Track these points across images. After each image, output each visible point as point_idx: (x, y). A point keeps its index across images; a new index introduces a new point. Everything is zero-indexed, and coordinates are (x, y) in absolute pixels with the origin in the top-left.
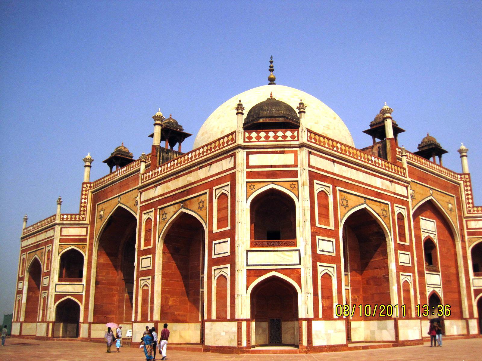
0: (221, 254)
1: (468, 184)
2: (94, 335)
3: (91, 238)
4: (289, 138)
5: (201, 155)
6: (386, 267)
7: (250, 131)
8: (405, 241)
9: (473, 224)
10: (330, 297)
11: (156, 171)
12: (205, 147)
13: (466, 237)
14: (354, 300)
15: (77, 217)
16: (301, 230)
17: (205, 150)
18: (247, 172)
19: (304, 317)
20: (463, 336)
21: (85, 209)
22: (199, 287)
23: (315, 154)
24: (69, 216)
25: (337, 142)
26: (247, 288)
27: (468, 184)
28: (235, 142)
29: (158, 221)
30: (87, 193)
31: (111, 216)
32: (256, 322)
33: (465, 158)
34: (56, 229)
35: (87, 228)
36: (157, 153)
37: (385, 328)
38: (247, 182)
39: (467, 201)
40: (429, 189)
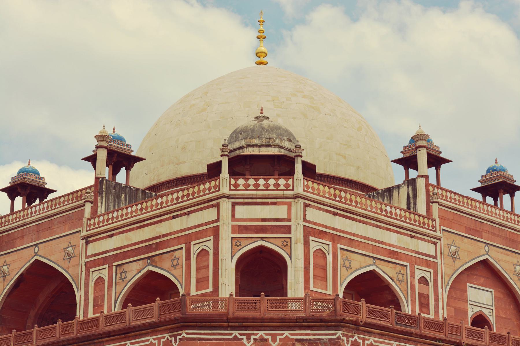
4: (282, 187)
5: (175, 202)
7: (237, 177)
11: (110, 216)
12: (181, 192)
28: (219, 190)
31: (22, 275)
38: (232, 238)
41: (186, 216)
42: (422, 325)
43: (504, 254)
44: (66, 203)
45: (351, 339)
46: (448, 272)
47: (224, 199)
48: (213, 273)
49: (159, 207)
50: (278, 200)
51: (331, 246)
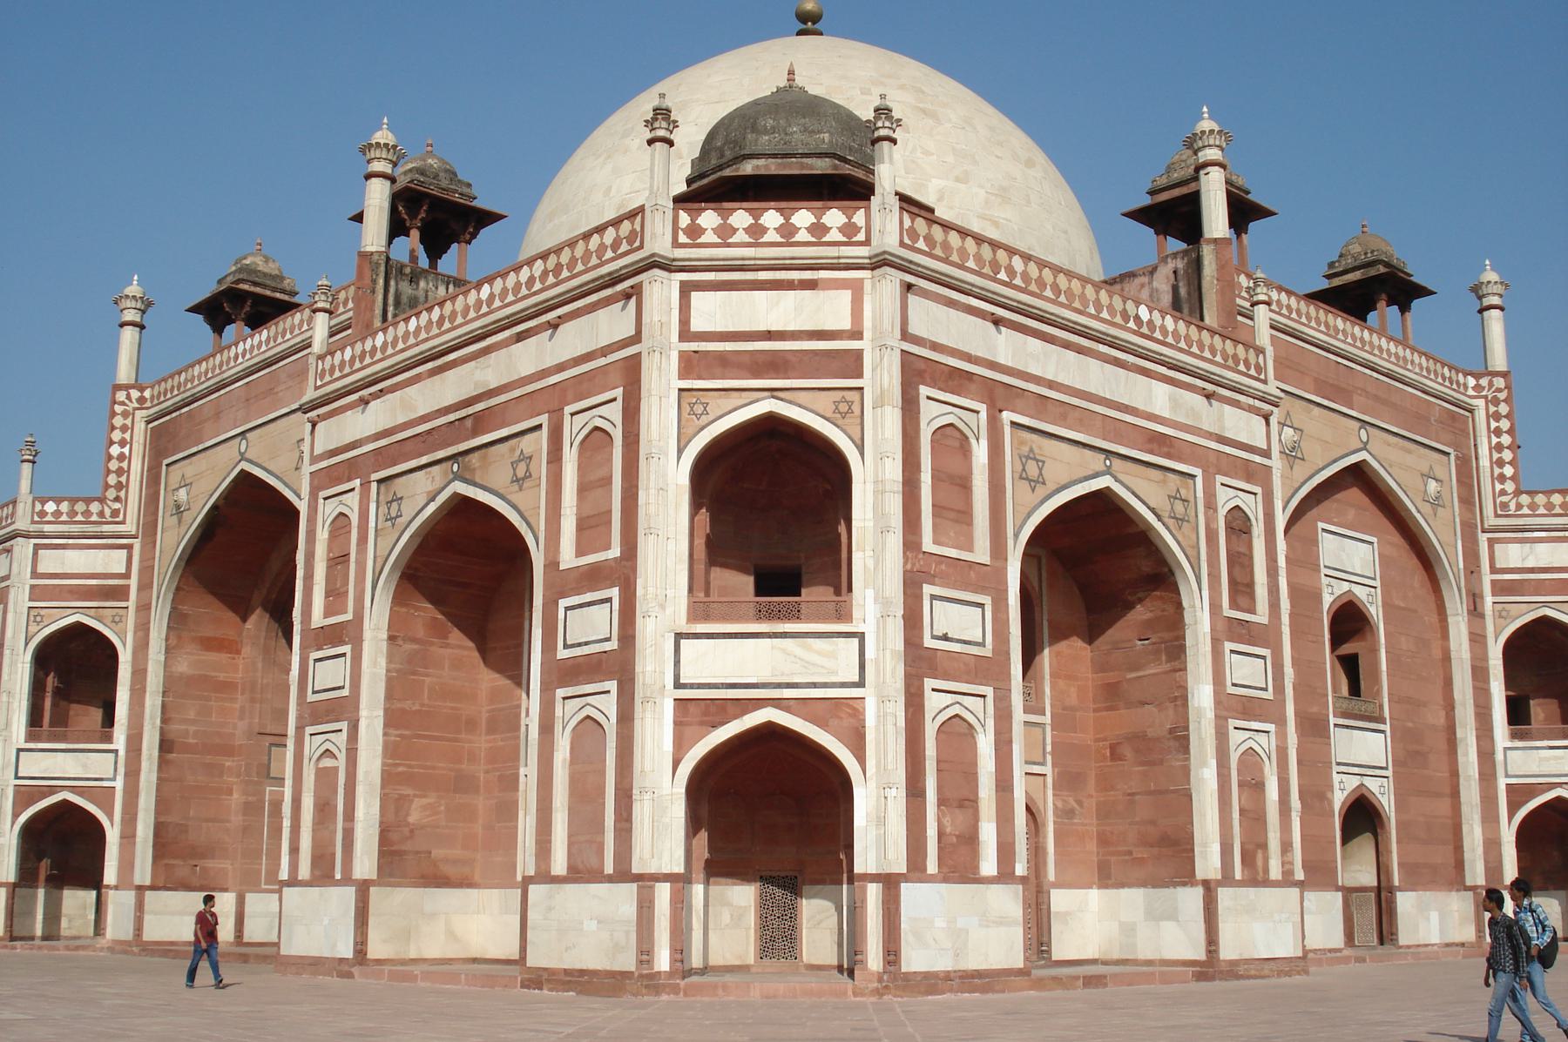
0: (586, 643)
2: (149, 935)
3: (145, 586)
4: (834, 235)
5: (524, 291)
6: (1181, 699)
7: (696, 205)
8: (1252, 611)
9: (1513, 555)
10: (969, 803)
11: (368, 345)
13: (1489, 599)
14: (1064, 814)
15: (95, 507)
16: (870, 563)
17: (537, 274)
18: (682, 354)
19: (872, 870)
20: (1461, 950)
21: (123, 479)
22: (517, 759)
23: (926, 294)
24: (64, 507)
25: (1012, 252)
26: (676, 764)
27: (1503, 409)
28: (641, 247)
29: (372, 524)
30: (128, 422)
31: (215, 507)
32: (707, 883)
33: (1495, 313)
34: (16, 550)
35: (129, 547)
36: (374, 282)
37: (1172, 916)
40: (1358, 425)
43: (1403, 449)
46: (1286, 489)
47: (656, 271)
48: (623, 499)
49: (484, 309)
50: (823, 274)
51: (983, 415)
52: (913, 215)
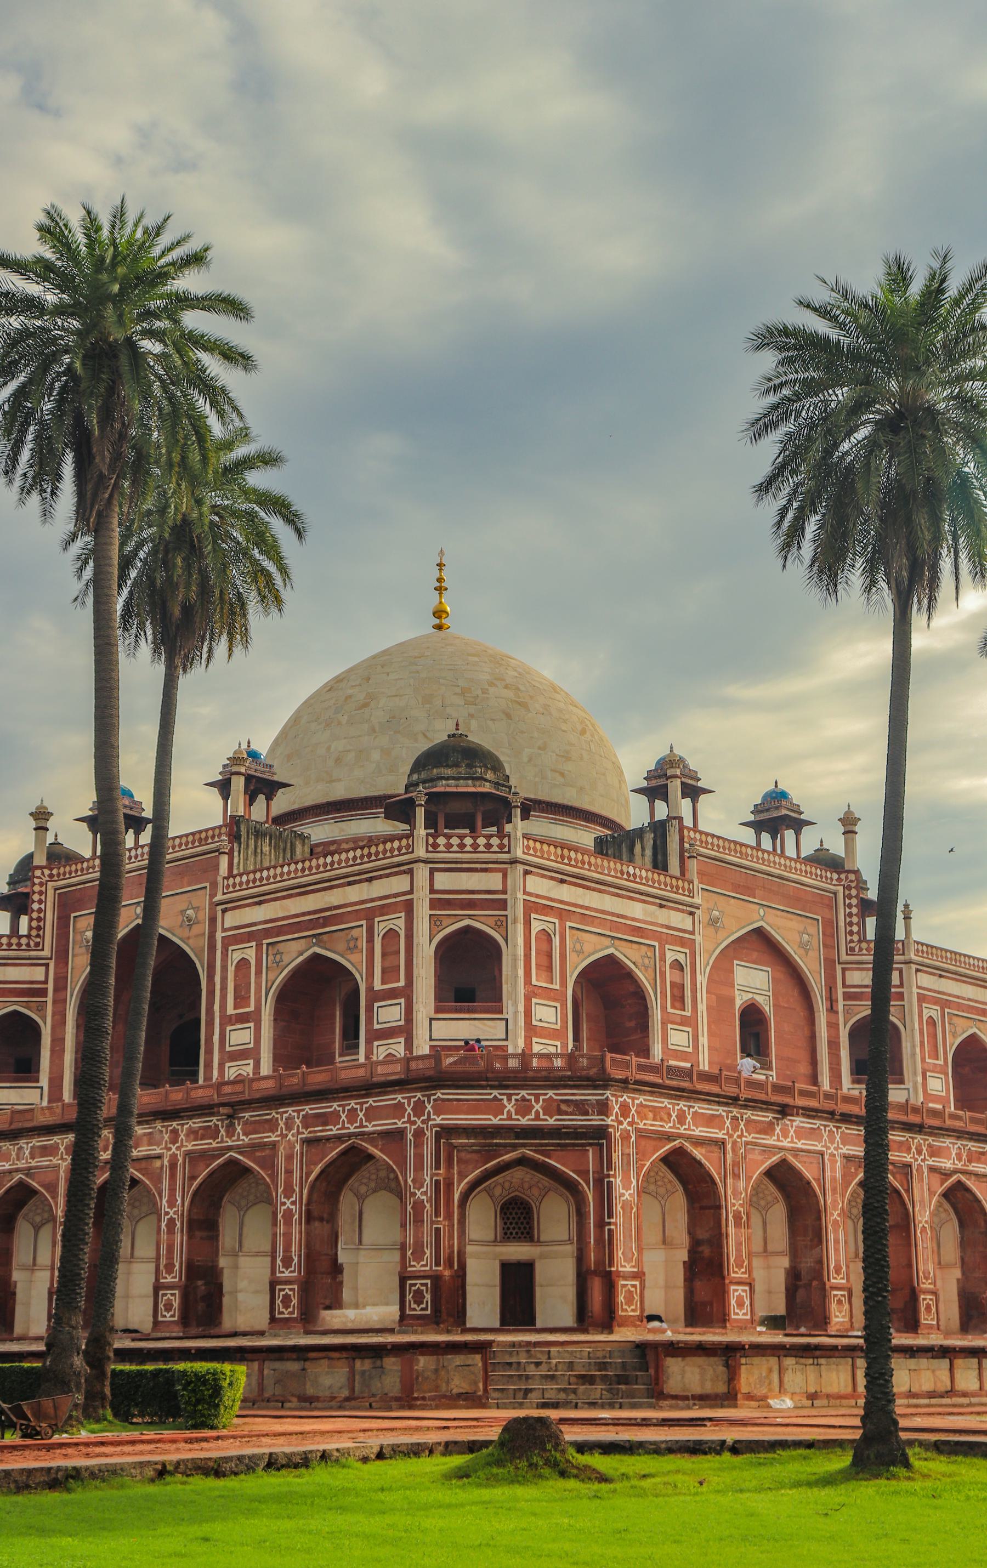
1: (854, 892)
4: (495, 849)
5: (351, 862)
15: (24, 941)
21: (41, 924)
28: (413, 852)
29: (264, 964)
33: (850, 835)
35: (47, 965)
39: (848, 929)
41: (366, 884)
42: (695, 1078)
43: (786, 918)
44: (183, 847)
45: (620, 1099)
46: (708, 947)
47: (422, 865)
49: (329, 868)
51: (557, 925)
52: (528, 839)
